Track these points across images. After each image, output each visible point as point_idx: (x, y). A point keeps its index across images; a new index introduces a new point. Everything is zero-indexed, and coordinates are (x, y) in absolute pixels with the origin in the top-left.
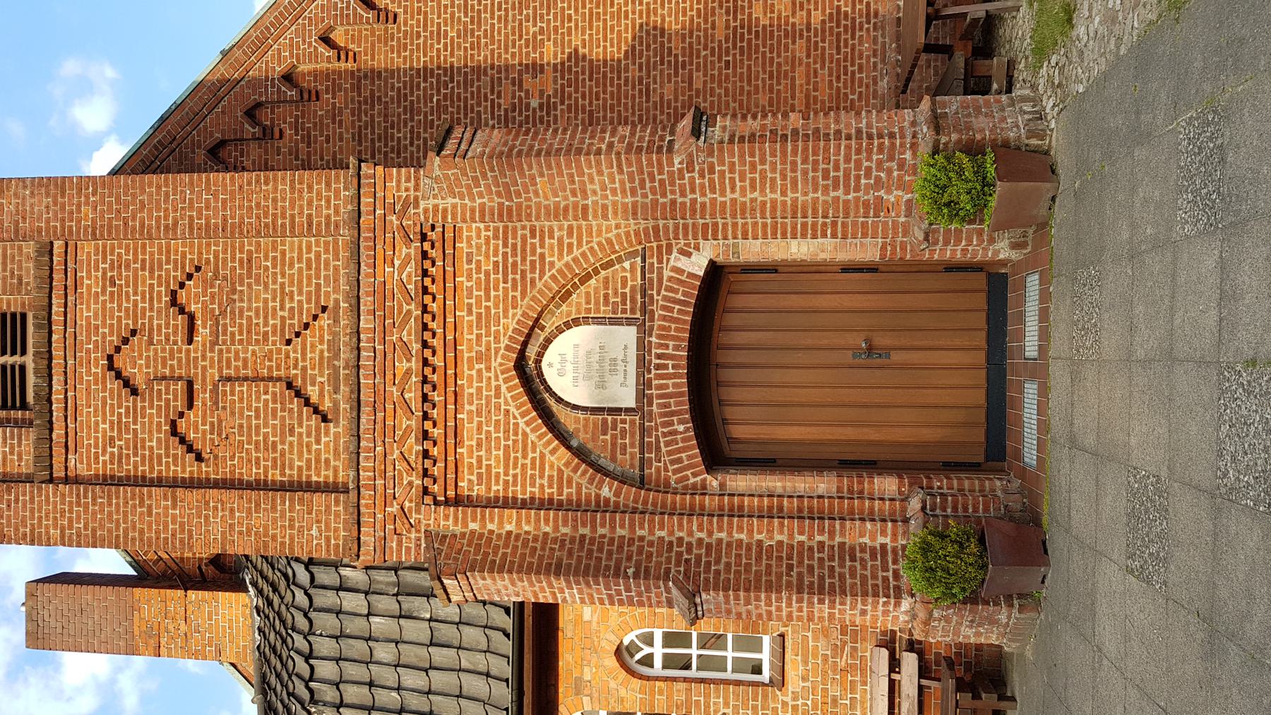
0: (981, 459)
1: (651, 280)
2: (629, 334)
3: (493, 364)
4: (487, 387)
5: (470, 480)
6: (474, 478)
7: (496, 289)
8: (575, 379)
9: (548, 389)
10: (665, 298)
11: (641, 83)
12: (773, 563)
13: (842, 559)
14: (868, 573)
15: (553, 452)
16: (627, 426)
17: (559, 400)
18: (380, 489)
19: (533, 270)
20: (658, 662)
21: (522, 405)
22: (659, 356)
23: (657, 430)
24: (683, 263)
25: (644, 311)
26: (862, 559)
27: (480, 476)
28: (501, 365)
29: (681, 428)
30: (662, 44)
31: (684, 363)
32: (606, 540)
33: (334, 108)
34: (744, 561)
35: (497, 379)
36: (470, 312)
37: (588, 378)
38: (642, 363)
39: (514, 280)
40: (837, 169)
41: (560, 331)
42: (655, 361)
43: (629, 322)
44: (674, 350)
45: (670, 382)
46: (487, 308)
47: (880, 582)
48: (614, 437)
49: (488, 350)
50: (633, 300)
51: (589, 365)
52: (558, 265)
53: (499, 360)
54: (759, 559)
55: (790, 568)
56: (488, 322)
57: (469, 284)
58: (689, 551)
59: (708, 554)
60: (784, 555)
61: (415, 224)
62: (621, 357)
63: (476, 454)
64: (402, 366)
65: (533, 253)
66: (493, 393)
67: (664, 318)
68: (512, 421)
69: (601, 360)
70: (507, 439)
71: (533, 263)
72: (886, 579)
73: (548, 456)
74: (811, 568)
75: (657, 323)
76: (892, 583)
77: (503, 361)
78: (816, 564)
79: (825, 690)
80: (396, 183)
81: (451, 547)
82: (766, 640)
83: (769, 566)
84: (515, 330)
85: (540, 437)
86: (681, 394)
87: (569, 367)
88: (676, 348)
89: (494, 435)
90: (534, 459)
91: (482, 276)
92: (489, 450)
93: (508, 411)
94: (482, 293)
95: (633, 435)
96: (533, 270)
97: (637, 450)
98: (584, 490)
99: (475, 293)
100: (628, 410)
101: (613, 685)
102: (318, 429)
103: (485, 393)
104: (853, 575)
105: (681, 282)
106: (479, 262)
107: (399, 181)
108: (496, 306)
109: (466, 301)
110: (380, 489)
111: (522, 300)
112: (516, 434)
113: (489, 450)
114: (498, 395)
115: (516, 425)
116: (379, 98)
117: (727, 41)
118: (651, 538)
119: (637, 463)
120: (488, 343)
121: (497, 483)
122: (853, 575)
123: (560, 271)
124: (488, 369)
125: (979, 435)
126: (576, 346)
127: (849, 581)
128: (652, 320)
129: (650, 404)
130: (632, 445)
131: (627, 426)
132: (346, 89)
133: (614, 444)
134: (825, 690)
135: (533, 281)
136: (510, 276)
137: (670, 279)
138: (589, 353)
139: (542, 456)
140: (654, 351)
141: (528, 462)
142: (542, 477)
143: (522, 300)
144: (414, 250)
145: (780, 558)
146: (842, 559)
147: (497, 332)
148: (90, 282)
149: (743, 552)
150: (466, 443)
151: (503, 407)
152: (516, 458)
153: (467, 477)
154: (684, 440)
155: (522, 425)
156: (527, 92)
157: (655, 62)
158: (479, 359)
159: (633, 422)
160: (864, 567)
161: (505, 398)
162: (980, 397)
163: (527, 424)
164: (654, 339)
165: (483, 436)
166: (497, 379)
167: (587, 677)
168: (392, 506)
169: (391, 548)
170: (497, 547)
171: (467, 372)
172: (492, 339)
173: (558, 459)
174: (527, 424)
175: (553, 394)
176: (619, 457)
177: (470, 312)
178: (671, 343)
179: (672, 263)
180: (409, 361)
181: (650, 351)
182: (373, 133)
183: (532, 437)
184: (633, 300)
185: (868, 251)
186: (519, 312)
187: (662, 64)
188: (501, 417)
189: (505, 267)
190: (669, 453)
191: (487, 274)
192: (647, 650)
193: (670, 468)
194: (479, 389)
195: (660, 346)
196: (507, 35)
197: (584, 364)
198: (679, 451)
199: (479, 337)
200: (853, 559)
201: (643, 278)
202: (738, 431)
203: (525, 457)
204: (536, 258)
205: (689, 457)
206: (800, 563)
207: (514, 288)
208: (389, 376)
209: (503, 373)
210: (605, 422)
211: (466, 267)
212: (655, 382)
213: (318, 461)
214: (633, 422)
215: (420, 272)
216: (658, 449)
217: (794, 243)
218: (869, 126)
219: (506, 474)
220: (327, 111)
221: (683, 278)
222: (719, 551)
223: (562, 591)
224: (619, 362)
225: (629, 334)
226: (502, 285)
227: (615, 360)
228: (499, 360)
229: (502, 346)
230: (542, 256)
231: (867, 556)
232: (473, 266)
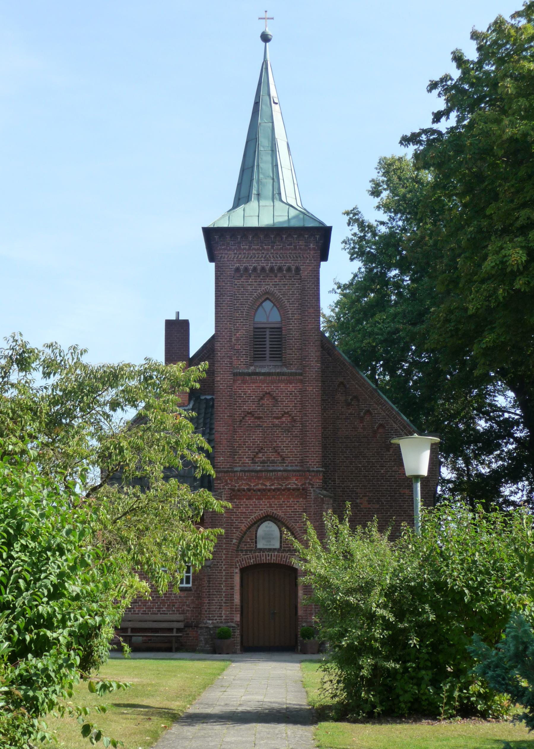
2: (277, 545)
4: (264, 507)
17: (259, 526)
38: (270, 550)
43: (281, 546)
44: (273, 558)
52: (296, 527)
64: (268, 484)
80: (318, 482)
87: (268, 529)
100: (256, 546)
148: (291, 387)
183: (249, 520)
194: (261, 505)
225: (277, 545)
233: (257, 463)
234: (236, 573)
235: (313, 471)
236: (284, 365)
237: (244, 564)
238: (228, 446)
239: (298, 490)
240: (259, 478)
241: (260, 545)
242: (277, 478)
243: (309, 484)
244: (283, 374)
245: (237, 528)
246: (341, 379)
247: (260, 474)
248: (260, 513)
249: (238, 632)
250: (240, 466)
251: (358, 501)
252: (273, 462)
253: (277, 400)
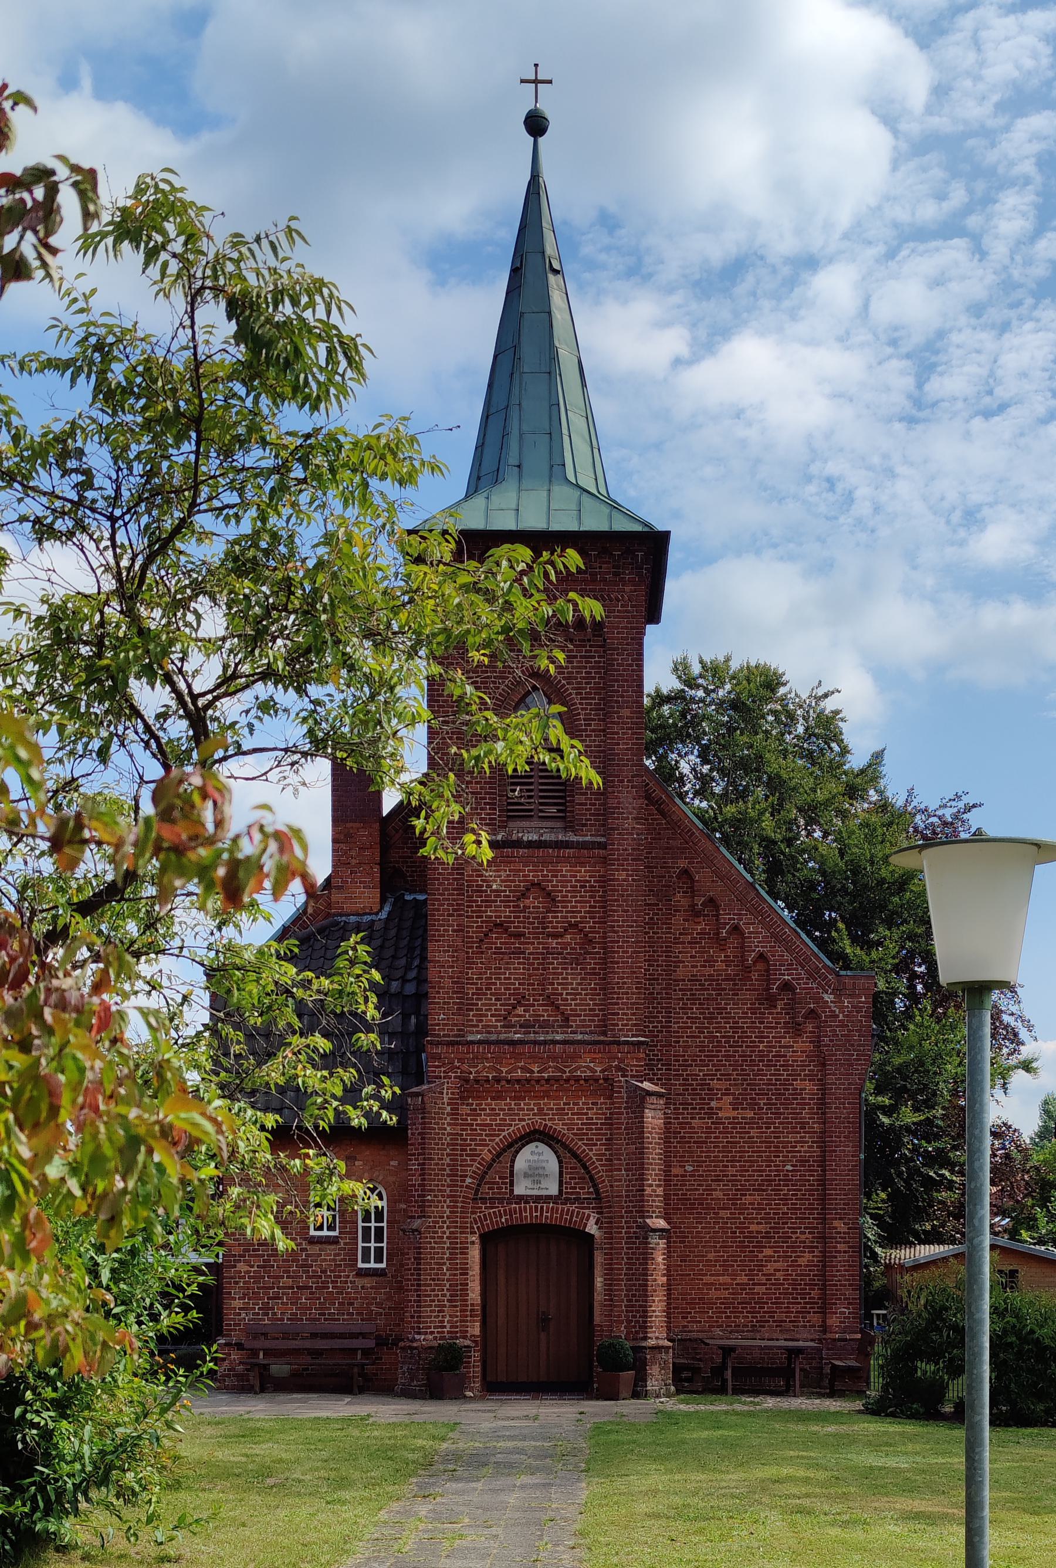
2: (554, 1190)
4: (527, 1114)
17: (517, 1152)
25: (567, 1199)
37: (530, 1167)
38: (538, 1199)
41: (556, 1153)
43: (560, 1191)
82: (383, 1265)
87: (536, 1158)
100: (512, 1191)
113: (489, 1115)
148: (583, 873)
158: (540, 1110)
225: (554, 1190)
233: (514, 1026)
234: (473, 1243)
235: (627, 1043)
236: (569, 826)
237: (489, 1226)
238: (454, 993)
239: (597, 1080)
240: (518, 1057)
241: (519, 1190)
242: (554, 1059)
243: (619, 1069)
244: (567, 845)
245: (473, 1156)
246: (683, 864)
247: (519, 1049)
248: (520, 1126)
249: (476, 1356)
250: (478, 1032)
251: (713, 1104)
252: (545, 1025)
253: (553, 900)
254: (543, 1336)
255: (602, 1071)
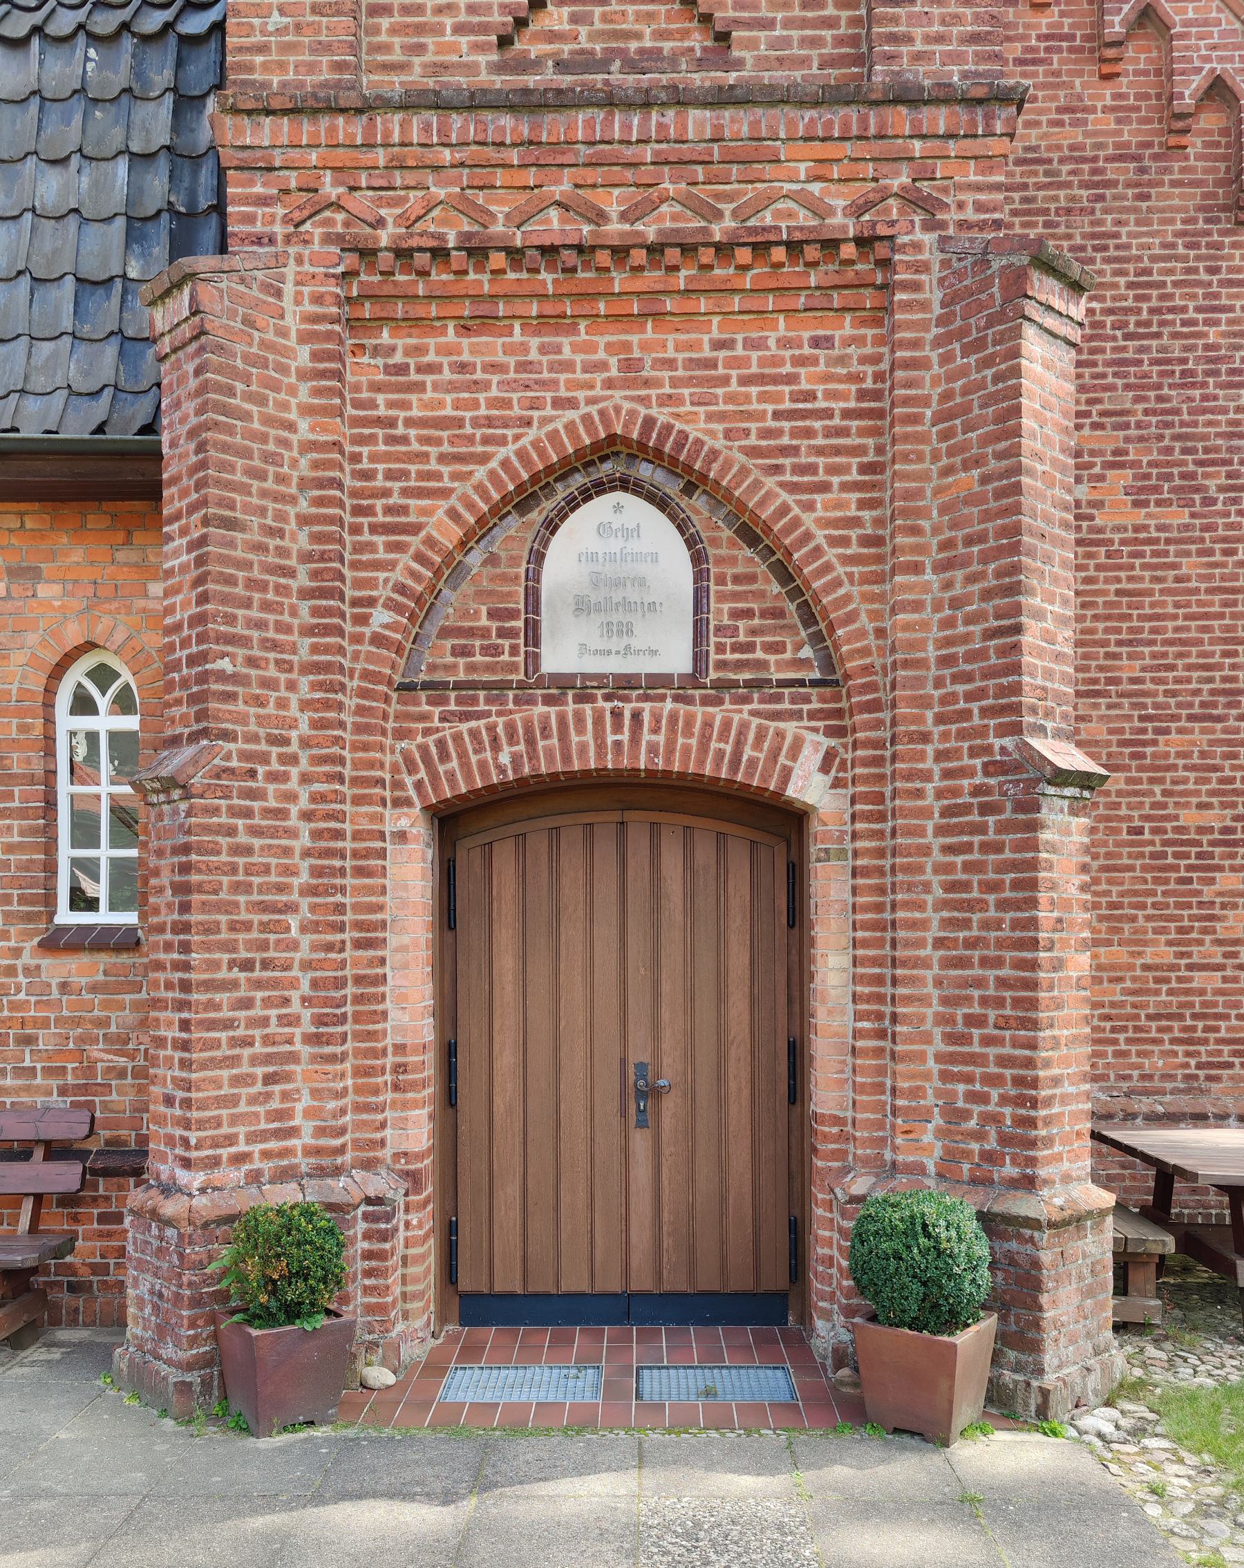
0: (466, 1283)
1: (778, 698)
3: (618, 394)
5: (393, 349)
6: (398, 358)
7: (762, 398)
8: (593, 557)
9: (573, 504)
10: (744, 726)
11: (1110, 681)
12: (255, 935)
13: (268, 1059)
14: (243, 1108)
15: (453, 514)
16: (506, 657)
17: (552, 526)
18: (366, 157)
19: (800, 469)
20: (85, 723)
21: (542, 453)
22: (636, 716)
23: (499, 714)
24: (810, 758)
25: (720, 685)
26: (268, 1096)
27: (402, 369)
28: (617, 409)
29: (505, 759)
30: (1175, 718)
31: (626, 763)
32: (286, 618)
33: (1085, 110)
34: (256, 880)
35: (591, 401)
36: (718, 345)
38: (625, 684)
39: (778, 433)
40: (987, 1041)
42: (627, 709)
43: (699, 658)
45: (589, 737)
46: (725, 381)
47: (225, 1130)
48: (484, 633)
49: (647, 383)
50: (740, 665)
51: (619, 583)
52: (808, 519)
53: (627, 405)
54: (264, 907)
55: (247, 966)
56: (701, 382)
57: (772, 343)
58: (273, 777)
59: (267, 813)
60: (271, 954)
61: (892, 224)
62: (636, 643)
63: (445, 360)
64: (613, 203)
65: (833, 470)
66: (563, 393)
67: (708, 725)
68: (509, 433)
69: (627, 605)
70: (476, 423)
71: (811, 469)
72: (231, 1140)
73: (444, 505)
74: (247, 1004)
75: (699, 711)
76: (225, 1152)
77: (625, 410)
78: (257, 1012)
79: (45, 1023)
81: (257, 304)
82: (130, 918)
83: (247, 926)
84: (684, 435)
85: (480, 489)
86: (566, 758)
87: (615, 545)
88: (653, 749)
89: (481, 397)
90: (438, 476)
91: (787, 369)
92: (452, 387)
93: (529, 423)
94: (754, 369)
95: (490, 668)
96: (800, 469)
97: (462, 676)
98: (382, 575)
99: (755, 355)
100: (533, 660)
101: (32, 638)
102: (483, 28)
103: (563, 377)
104: (236, 1081)
105: (774, 755)
106: (814, 361)
107: (979, 188)
108: (730, 398)
109: (739, 338)
110: (366, 157)
111: (741, 449)
112: (486, 441)
113: (452, 387)
114: (558, 403)
115: (503, 441)
116: (1101, 198)
117: (1177, 830)
118: (294, 704)
119: (439, 676)
120: (658, 383)
121: (391, 405)
122: (236, 1081)
123: (796, 523)
124: (609, 384)
125: (508, 1281)
126: (655, 558)
127: (225, 1074)
128: (706, 701)
129: (549, 700)
130: (471, 668)
131: (506, 657)
132: (1119, 133)
133: (471, 633)
134: (45, 1023)
135: (777, 469)
136: (786, 425)
137: (780, 735)
138: (642, 582)
139: (445, 493)
140: (647, 706)
141: (433, 466)
142: (405, 492)
143: (741, 449)
144: (841, 222)
145: (264, 946)
146: (268, 1059)
147: (680, 401)
149: (273, 878)
150: (465, 342)
151: (536, 414)
152: (438, 442)
153: (400, 342)
154: (483, 765)
155: (502, 452)
156: (1101, 478)
157: (1144, 706)
158: (629, 365)
159: (513, 667)
160: (253, 1100)
161: (551, 419)
162: (575, 1281)
163: (505, 464)
164: (669, 705)
165: (479, 375)
166: (591, 401)
167: (44, 591)
168: (336, 183)
169: (251, 183)
170: (262, 401)
171: (602, 340)
172: (667, 390)
173: (440, 521)
174: (505, 464)
175: (563, 515)
176: (448, 643)
177: (718, 345)
178: (661, 738)
179: (810, 736)
180: (623, 217)
181: (646, 698)
182: (1039, 187)
183: (480, 472)
184: (740, 665)
185: (828, 1093)
186: (719, 444)
187: (1142, 718)
188: (517, 411)
189: (805, 414)
190: (457, 738)
191: (791, 379)
192: (103, 702)
193: (431, 740)
194: (568, 366)
195: (657, 719)
196: (1205, 437)
197: (619, 592)
198: (463, 755)
199: (670, 364)
200: (269, 1079)
201: (783, 684)
202: (504, 857)
203: (442, 458)
204: (821, 476)
205: (451, 776)
206: (258, 985)
207: (766, 433)
208: (596, 176)
209: (602, 413)
210: (512, 614)
211: (806, 335)
212: (587, 707)
213: (420, 29)
214: (513, 667)
215: (798, 236)
216: (465, 717)
217: (846, 961)
218: (1065, 1099)
219: (409, 422)
220: (1080, 98)
221: (782, 760)
222: (274, 833)
223: (184, 532)
224: (625, 640)
226: (770, 408)
227: (630, 632)
228: (627, 405)
229: (654, 411)
230: (824, 487)
231: (275, 1104)
232: (807, 350)
240: (544, 156)
254: (640, 1141)
255: (857, 210)
